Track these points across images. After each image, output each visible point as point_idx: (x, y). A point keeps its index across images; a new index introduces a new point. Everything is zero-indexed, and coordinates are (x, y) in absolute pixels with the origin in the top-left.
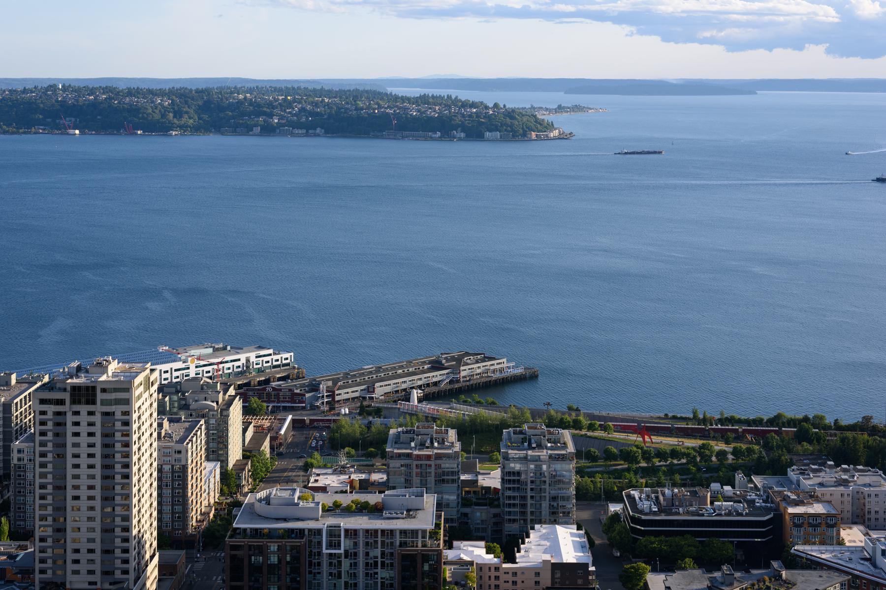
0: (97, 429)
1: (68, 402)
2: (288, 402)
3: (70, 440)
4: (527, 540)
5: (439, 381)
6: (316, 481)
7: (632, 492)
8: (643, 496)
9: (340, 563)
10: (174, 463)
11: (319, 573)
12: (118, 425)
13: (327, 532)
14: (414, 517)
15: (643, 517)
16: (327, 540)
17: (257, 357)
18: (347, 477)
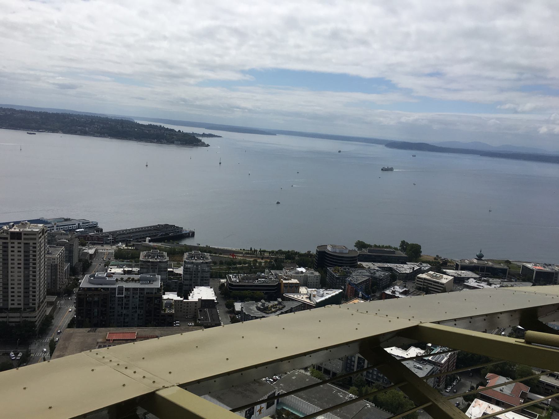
0: (22, 250)
1: (9, 238)
2: (96, 241)
3: (10, 253)
4: (192, 292)
5: (157, 235)
6: (110, 271)
7: (230, 275)
8: (234, 276)
9: (122, 300)
10: (52, 263)
11: (114, 304)
12: (31, 248)
13: (118, 288)
14: (152, 284)
15: (234, 284)
16: (118, 292)
17: (83, 223)
18: (123, 269)
